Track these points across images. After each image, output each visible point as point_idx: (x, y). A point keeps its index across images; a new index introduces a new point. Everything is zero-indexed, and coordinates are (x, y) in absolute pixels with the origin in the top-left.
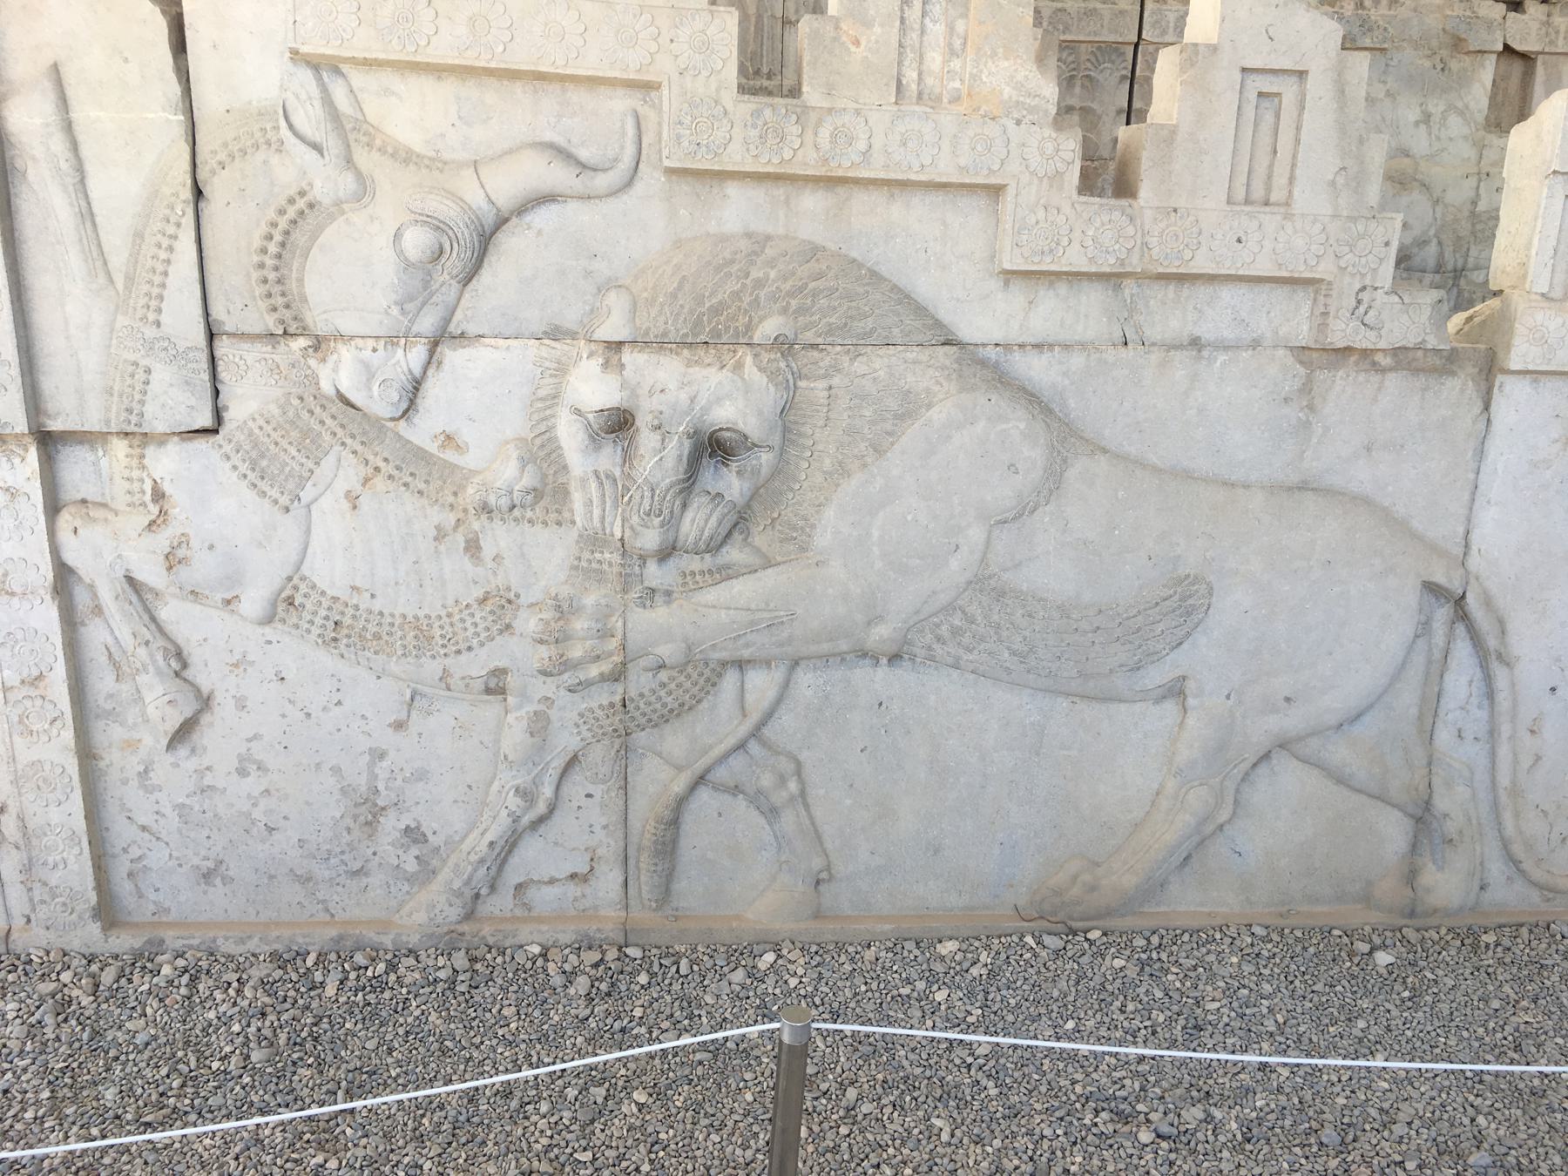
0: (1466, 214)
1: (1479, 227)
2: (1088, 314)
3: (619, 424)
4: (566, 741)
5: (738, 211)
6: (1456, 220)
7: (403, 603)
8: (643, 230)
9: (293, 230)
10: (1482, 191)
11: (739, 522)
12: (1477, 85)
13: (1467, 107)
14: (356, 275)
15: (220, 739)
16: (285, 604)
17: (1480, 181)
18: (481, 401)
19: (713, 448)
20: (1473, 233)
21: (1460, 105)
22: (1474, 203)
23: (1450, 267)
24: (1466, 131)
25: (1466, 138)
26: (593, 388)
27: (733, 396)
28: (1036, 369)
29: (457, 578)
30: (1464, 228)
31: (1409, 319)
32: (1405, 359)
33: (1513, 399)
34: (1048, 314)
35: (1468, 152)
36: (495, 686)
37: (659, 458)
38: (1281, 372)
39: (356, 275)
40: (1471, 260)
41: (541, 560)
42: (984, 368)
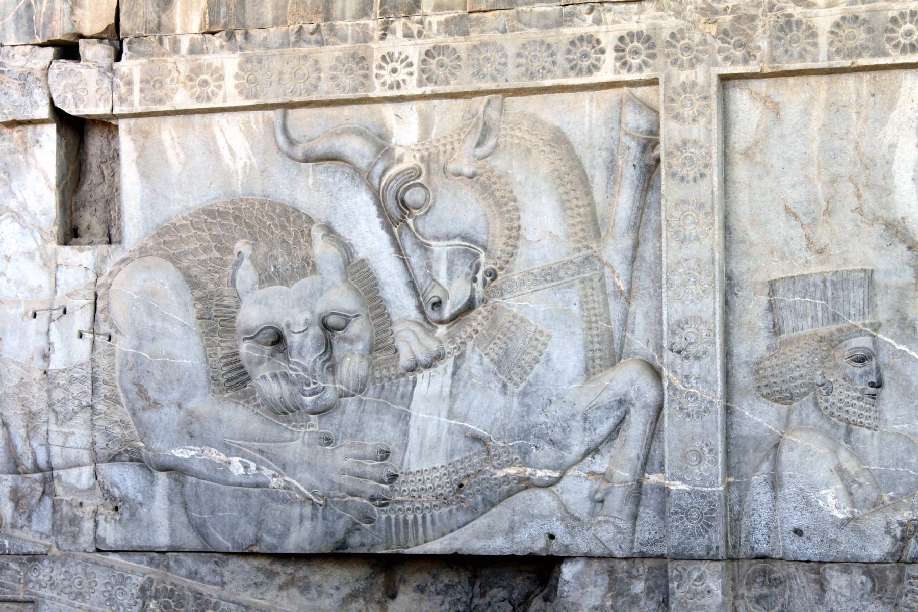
0: (38, 375)
1: (57, 395)
6: (23, 384)
10: (54, 337)
12: (34, 173)
13: (24, 207)
17: (51, 320)
20: (50, 406)
21: (13, 204)
22: (46, 357)
23: (28, 463)
24: (30, 244)
25: (30, 255)
30: (37, 399)
35: (38, 278)
40: (55, 450)
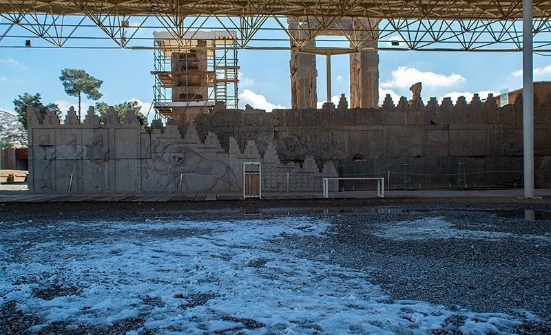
2: (202, 150)
3: (174, 157)
4: (171, 178)
5: (181, 145)
7: (161, 169)
8: (176, 146)
9: (156, 146)
11: (182, 163)
14: (159, 149)
15: (149, 179)
16: (154, 168)
18: (166, 156)
19: (180, 159)
26: (173, 155)
27: (181, 155)
28: (201, 154)
29: (165, 167)
31: (223, 150)
32: (223, 152)
33: (230, 155)
34: (200, 150)
36: (167, 174)
37: (177, 159)
38: (215, 154)
39: (159, 149)
41: (170, 166)
42: (196, 153)
